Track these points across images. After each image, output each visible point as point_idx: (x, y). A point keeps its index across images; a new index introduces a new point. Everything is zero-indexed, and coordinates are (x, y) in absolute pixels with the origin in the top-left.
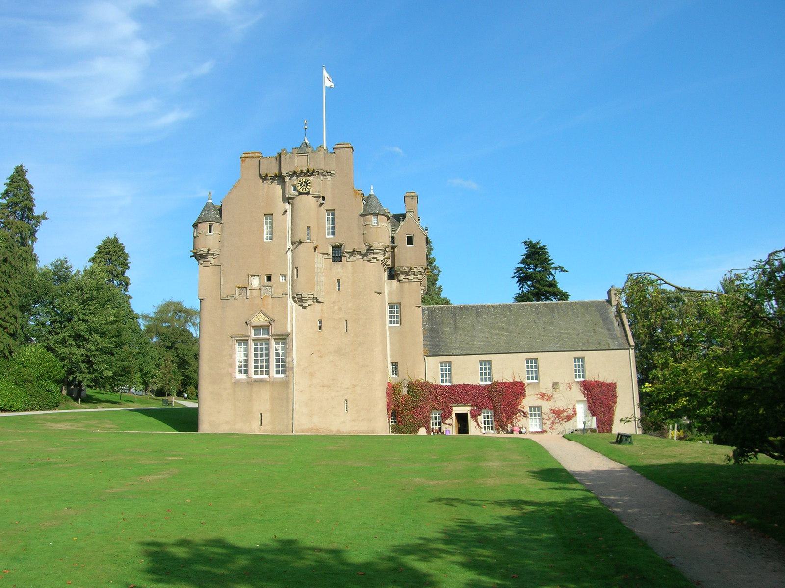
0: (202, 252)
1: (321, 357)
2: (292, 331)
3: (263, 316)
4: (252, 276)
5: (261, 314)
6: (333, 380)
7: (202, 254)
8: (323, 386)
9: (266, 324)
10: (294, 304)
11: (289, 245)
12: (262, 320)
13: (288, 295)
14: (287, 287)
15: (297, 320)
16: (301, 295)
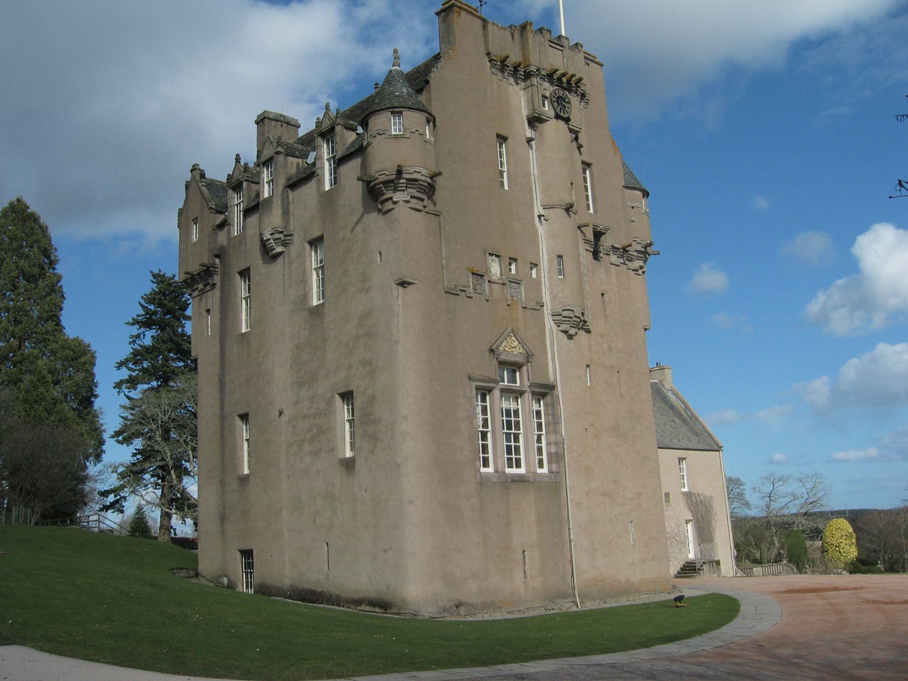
0: (415, 176)
1: (596, 437)
2: (555, 379)
3: (516, 343)
4: (491, 254)
5: (514, 338)
6: (614, 482)
7: (417, 180)
8: (604, 495)
9: (520, 359)
10: (554, 327)
11: (538, 209)
12: (512, 349)
13: (545, 307)
14: (541, 290)
15: (561, 362)
16: (573, 311)
